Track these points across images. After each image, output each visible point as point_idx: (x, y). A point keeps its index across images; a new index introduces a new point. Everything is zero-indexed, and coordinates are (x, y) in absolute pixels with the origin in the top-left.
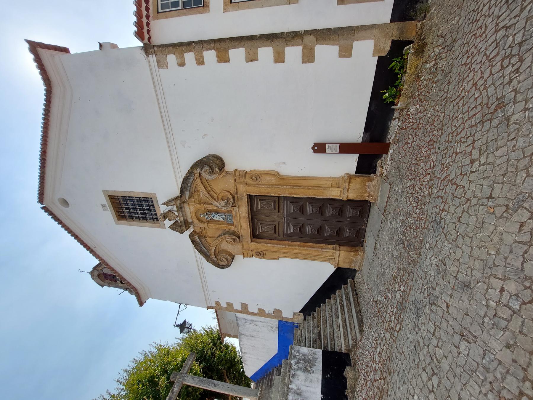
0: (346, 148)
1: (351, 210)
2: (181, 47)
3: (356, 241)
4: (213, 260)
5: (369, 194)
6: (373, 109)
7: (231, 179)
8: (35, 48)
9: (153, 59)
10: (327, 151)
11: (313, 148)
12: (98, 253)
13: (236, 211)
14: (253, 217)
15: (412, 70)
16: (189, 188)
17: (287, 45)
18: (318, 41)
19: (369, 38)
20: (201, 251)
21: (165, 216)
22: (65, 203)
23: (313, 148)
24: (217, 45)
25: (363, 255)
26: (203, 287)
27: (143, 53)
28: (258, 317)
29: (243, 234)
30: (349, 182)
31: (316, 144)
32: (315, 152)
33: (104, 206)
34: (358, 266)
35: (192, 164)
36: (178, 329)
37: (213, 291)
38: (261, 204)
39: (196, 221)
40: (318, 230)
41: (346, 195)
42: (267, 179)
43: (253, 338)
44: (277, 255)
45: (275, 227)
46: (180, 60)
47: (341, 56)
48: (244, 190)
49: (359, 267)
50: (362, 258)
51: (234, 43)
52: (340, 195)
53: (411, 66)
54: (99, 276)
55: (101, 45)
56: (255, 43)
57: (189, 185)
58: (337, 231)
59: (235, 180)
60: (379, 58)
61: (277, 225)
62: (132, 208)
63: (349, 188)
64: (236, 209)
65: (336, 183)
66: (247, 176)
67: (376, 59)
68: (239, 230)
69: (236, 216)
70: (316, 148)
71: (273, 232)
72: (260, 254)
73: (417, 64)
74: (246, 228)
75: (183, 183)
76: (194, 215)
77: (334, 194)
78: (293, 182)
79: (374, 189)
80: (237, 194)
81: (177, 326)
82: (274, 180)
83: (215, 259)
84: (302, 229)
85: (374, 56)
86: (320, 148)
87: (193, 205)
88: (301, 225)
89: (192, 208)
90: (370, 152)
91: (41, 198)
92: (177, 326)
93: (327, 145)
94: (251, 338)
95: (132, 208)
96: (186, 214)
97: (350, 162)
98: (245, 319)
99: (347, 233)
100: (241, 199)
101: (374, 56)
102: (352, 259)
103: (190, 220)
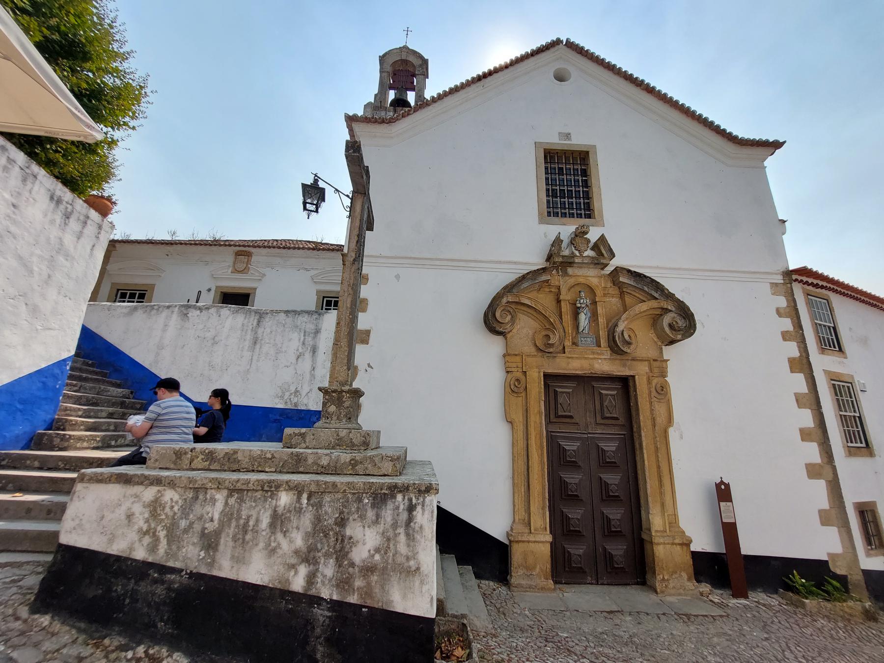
0: (730, 531)
1: (621, 553)
2: (793, 313)
3: (564, 570)
4: (503, 297)
5: (668, 580)
6: (773, 562)
7: (652, 353)
8: (777, 145)
9: (779, 279)
10: (722, 504)
11: (722, 482)
12: (473, 86)
13: (603, 354)
14: (586, 382)
15: (847, 610)
16: (639, 286)
17: (819, 445)
18: (829, 483)
19: (843, 547)
20: (524, 278)
21: (580, 234)
22: (560, 77)
23: (722, 482)
24: (805, 361)
25: (549, 589)
26: (410, 258)
27: (783, 269)
28: (328, 365)
29: (558, 360)
30: (681, 544)
31: (727, 486)
32: (718, 486)
33: (568, 136)
34: (523, 582)
35: (688, 303)
36: (309, 181)
37: (398, 277)
38: (611, 395)
39: (572, 281)
40: (577, 496)
41: (662, 540)
42: (660, 409)
43: (247, 344)
44: (519, 418)
45: (571, 417)
46: (782, 311)
47: (821, 512)
48: (640, 372)
49: (519, 586)
50: (543, 589)
51: (810, 380)
52: (657, 531)
53: (851, 608)
54: (405, 62)
55: (784, 222)
56: (814, 407)
57: (646, 289)
58: (579, 532)
59: (655, 360)
60: (827, 562)
61: (573, 421)
62: (568, 180)
63: (673, 544)
64: (607, 354)
65: (674, 522)
66: (661, 379)
67: (825, 558)
68: (567, 354)
69: (593, 353)
70: (723, 487)
71: (560, 413)
72: (515, 388)
73: (855, 616)
74: (570, 366)
75: (653, 281)
76: (581, 280)
77: (656, 521)
78: (662, 451)
79: (677, 586)
80: (634, 360)
81: (316, 181)
82: (661, 420)
83: (504, 300)
84: (573, 465)
85: (829, 554)
86: (723, 492)
87: (600, 283)
88: (580, 463)
89: (594, 281)
90: (726, 569)
91: (570, 45)
92: (316, 181)
93: (729, 504)
94: (249, 337)
95: (568, 180)
96: (581, 267)
97: (704, 541)
98: (317, 332)
99: (577, 550)
100: (624, 365)
101: (829, 554)
102: (534, 568)
103: (570, 271)
